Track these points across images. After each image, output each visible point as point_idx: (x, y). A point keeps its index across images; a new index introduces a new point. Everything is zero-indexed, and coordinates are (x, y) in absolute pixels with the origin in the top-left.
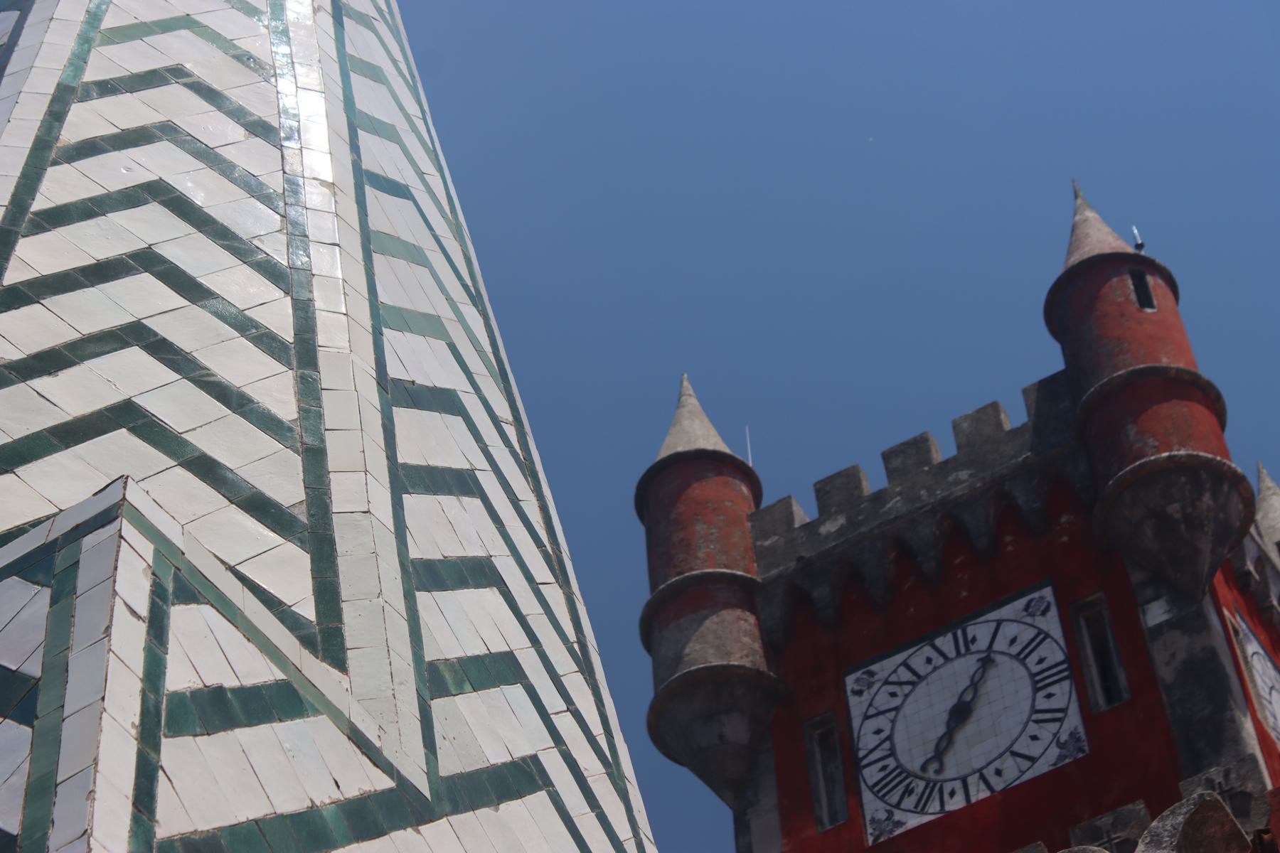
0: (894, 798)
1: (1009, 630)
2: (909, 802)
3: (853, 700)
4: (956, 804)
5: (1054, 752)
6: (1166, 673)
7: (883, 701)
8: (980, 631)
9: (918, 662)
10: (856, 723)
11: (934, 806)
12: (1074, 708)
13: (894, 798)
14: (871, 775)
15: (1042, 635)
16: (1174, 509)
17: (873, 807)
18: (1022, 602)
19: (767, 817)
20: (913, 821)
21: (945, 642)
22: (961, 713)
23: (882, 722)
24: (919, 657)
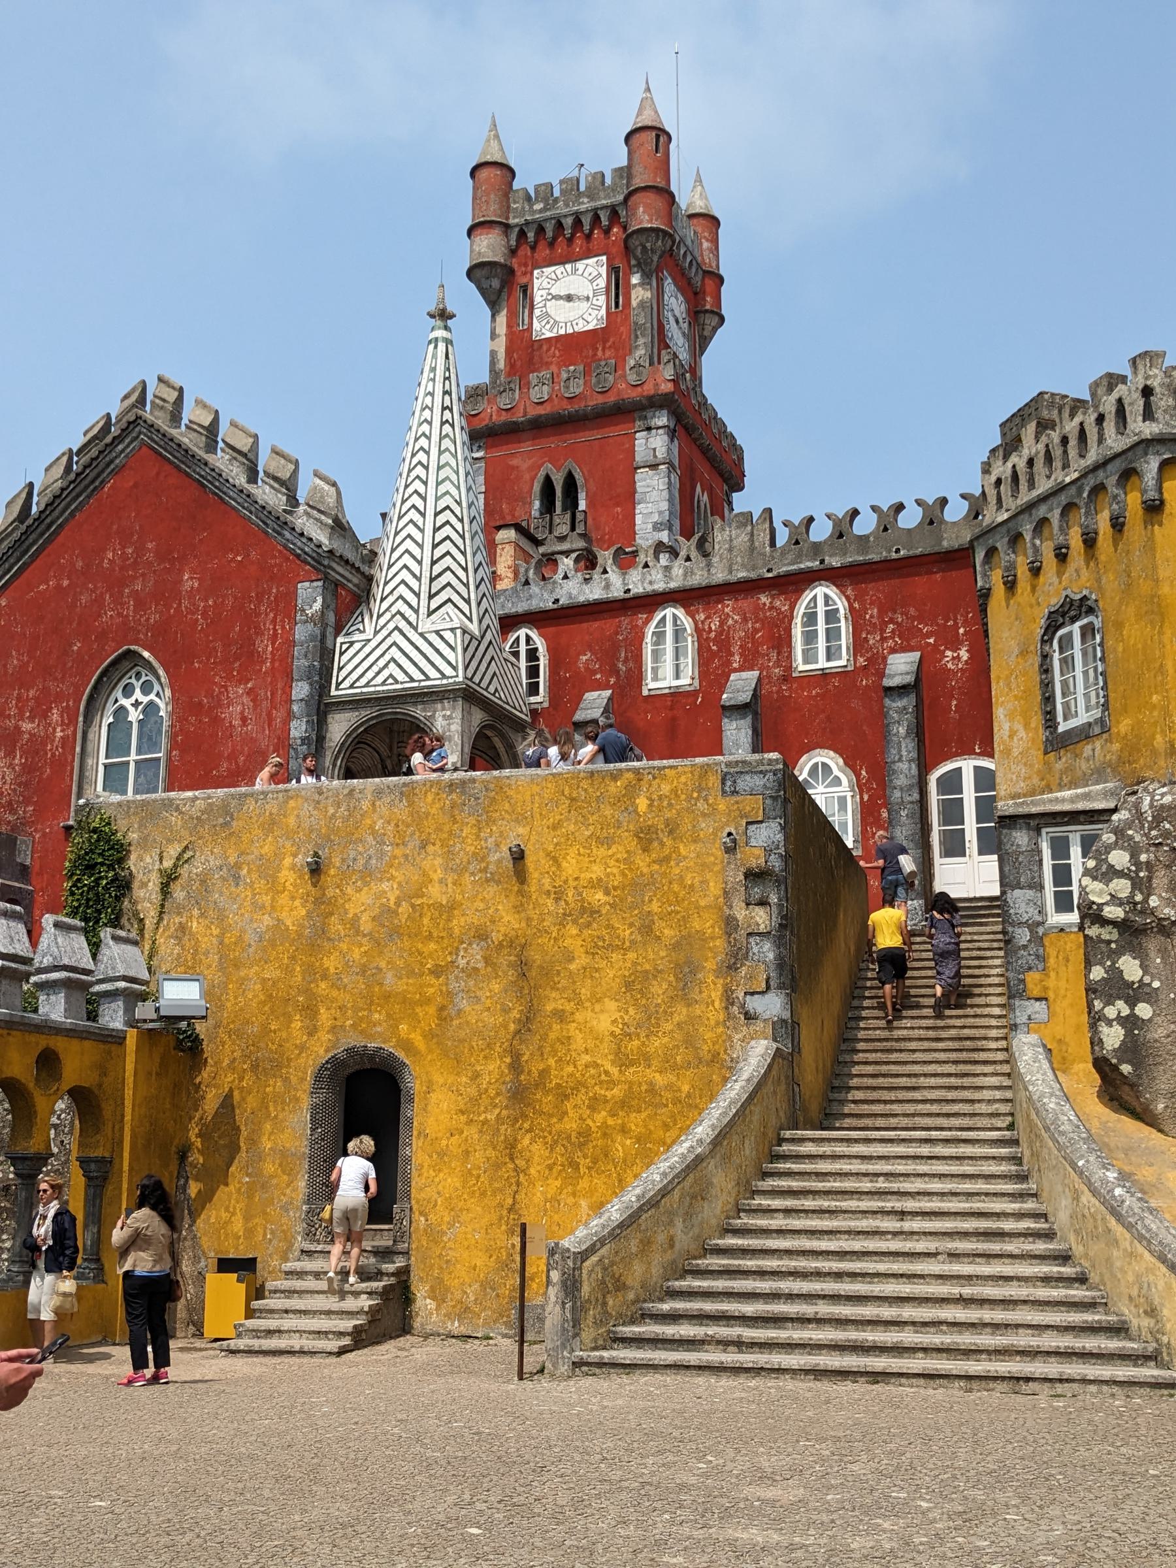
0: (543, 323)
1: (590, 269)
2: (548, 327)
3: (535, 281)
4: (562, 332)
5: (595, 322)
6: (634, 303)
7: (545, 285)
8: (580, 265)
9: (558, 272)
10: (535, 290)
11: (555, 330)
12: (604, 307)
13: (543, 323)
14: (537, 312)
15: (600, 275)
16: (648, 245)
17: (536, 325)
18: (595, 259)
19: (502, 319)
20: (548, 335)
21: (568, 266)
22: (569, 298)
23: (544, 292)
24: (559, 269)
